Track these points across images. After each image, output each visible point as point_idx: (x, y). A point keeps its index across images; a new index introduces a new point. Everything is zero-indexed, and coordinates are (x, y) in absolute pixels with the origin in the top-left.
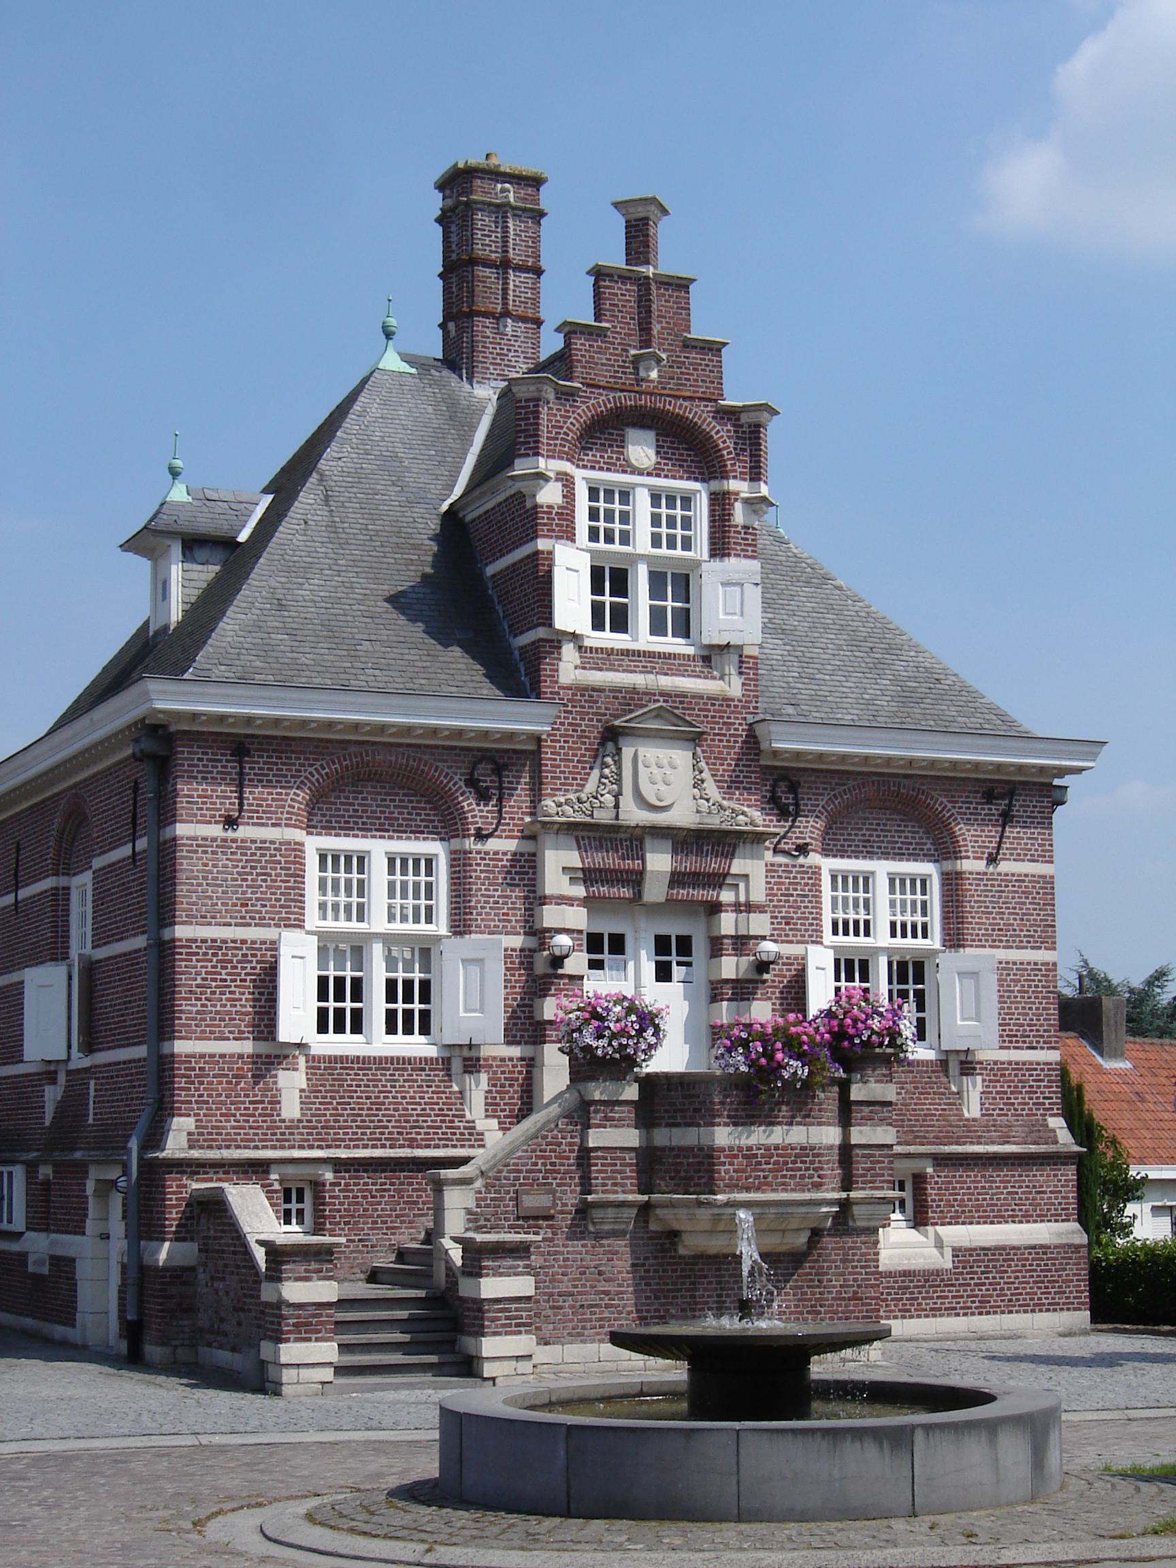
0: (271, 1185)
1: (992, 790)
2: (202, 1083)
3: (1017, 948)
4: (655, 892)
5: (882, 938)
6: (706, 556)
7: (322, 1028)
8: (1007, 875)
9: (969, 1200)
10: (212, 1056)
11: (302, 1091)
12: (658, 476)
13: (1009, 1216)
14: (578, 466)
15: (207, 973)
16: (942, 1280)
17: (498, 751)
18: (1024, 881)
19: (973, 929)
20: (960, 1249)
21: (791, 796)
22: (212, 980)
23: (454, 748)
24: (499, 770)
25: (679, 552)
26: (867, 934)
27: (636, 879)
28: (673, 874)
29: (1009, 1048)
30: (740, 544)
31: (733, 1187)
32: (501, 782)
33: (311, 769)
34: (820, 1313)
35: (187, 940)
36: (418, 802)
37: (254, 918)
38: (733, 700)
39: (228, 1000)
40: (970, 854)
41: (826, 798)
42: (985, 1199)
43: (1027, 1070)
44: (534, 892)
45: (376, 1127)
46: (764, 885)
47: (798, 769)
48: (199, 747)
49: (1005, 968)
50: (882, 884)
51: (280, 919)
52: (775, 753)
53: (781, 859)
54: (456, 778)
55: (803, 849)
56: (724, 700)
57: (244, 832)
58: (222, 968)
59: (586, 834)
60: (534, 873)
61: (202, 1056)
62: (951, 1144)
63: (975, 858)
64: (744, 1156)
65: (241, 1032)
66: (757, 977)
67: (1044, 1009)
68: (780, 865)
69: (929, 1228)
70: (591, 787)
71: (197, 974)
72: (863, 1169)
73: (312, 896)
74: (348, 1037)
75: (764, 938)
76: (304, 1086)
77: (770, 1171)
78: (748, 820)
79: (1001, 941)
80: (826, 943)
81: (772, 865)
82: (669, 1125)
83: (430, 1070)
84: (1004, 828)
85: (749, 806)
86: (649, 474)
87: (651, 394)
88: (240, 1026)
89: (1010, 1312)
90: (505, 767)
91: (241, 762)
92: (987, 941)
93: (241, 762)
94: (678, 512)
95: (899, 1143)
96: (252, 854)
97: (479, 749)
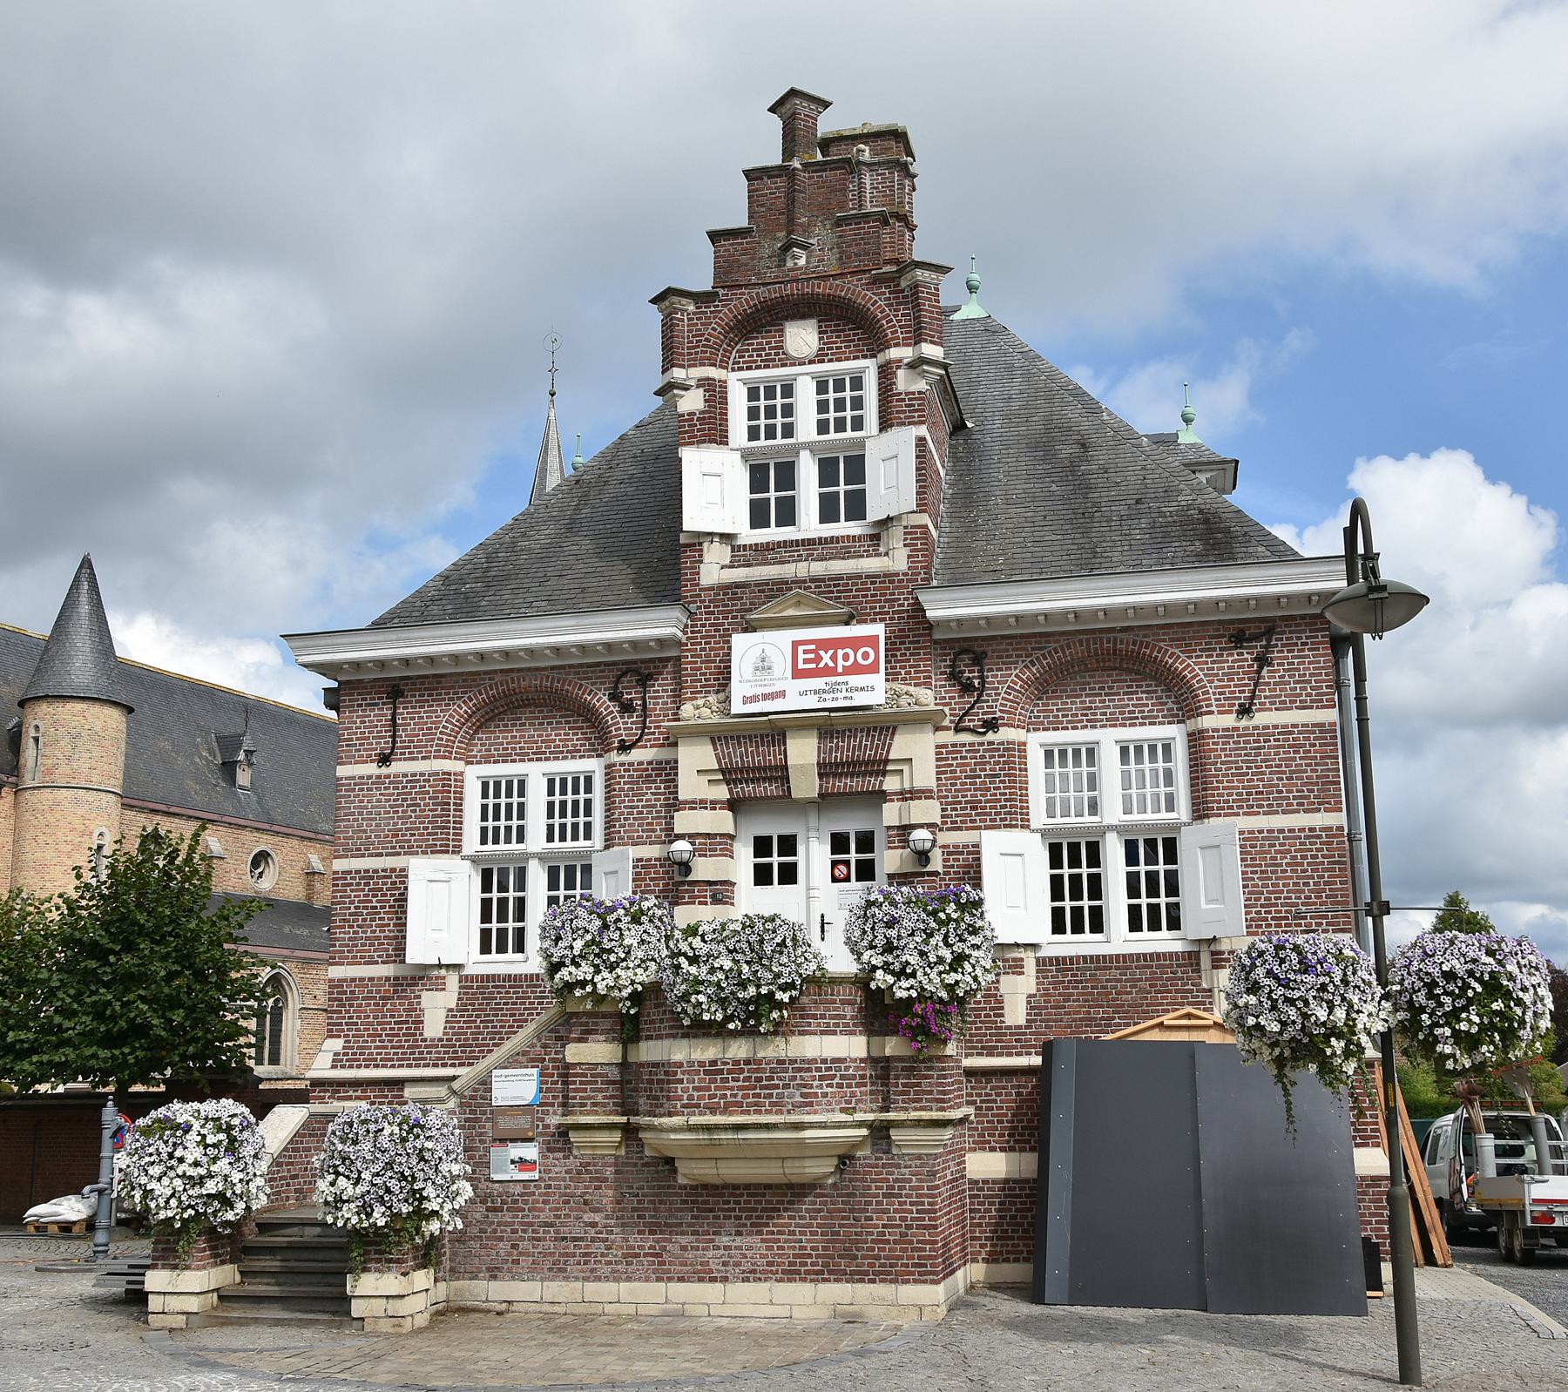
1: (1242, 631)
3: (1284, 812)
4: (805, 785)
11: (450, 1010)
12: (822, 361)
17: (643, 661)
18: (1291, 733)
23: (598, 664)
25: (849, 434)
27: (781, 773)
31: (692, 1106)
34: (856, 1257)
40: (1214, 708)
41: (1021, 665)
47: (984, 639)
49: (1248, 838)
50: (1109, 757)
52: (945, 623)
53: (966, 738)
55: (991, 725)
56: (885, 575)
57: (397, 767)
61: (353, 980)
63: (1220, 713)
64: (706, 1072)
67: (1326, 883)
71: (352, 902)
76: (453, 1006)
82: (649, 1038)
85: (916, 685)
86: (811, 362)
87: (797, 281)
90: (650, 677)
91: (394, 703)
92: (1241, 807)
93: (394, 703)
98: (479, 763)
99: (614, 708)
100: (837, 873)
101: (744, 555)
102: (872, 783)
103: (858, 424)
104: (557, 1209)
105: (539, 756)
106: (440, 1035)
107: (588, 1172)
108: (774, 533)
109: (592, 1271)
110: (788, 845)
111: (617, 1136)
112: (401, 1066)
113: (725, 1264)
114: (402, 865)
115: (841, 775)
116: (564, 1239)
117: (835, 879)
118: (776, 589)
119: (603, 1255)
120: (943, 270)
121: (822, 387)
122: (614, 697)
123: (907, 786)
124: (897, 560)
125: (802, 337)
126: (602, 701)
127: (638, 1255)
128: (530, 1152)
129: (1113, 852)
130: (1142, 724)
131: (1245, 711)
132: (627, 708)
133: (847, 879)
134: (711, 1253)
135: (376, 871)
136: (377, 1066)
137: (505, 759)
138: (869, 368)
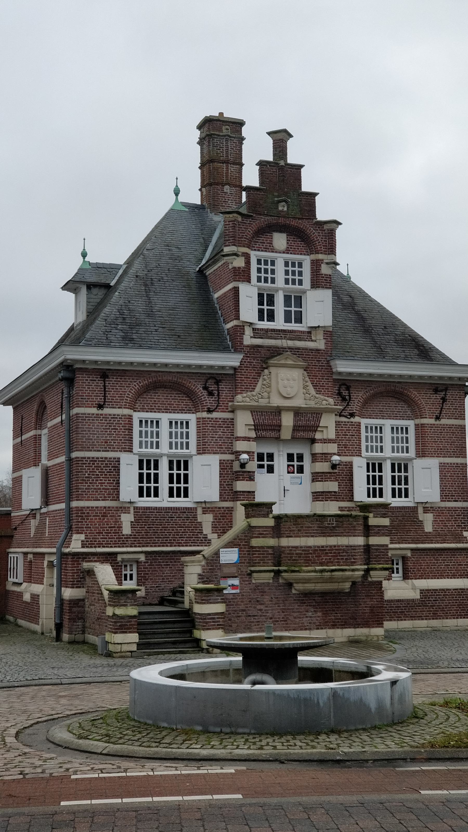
0: (118, 563)
2: (88, 519)
3: (449, 457)
4: (286, 434)
5: (387, 453)
6: (309, 287)
7: (141, 495)
8: (444, 425)
9: (427, 568)
10: (92, 507)
11: (132, 522)
12: (288, 253)
13: (446, 575)
14: (252, 250)
15: (90, 472)
16: (415, 604)
17: (217, 374)
19: (429, 449)
20: (423, 590)
21: (347, 392)
22: (93, 475)
24: (217, 382)
25: (297, 286)
26: (382, 451)
27: (278, 428)
28: (294, 426)
29: (445, 501)
30: (324, 282)
32: (218, 388)
33: (135, 383)
35: (81, 458)
36: (182, 397)
37: (110, 448)
38: (321, 350)
39: (99, 483)
41: (363, 392)
42: (434, 568)
43: (454, 511)
44: (233, 435)
45: (164, 538)
46: (335, 431)
48: (86, 375)
51: (122, 448)
52: (340, 373)
54: (199, 386)
55: (352, 415)
57: (106, 411)
58: (97, 469)
59: (254, 411)
60: (233, 427)
61: (88, 507)
62: (419, 543)
65: (104, 497)
66: (332, 471)
67: (461, 484)
68: (342, 422)
69: (410, 581)
70: (258, 389)
71: (86, 472)
72: (375, 555)
73: (136, 439)
74: (152, 498)
75: (335, 454)
76: (133, 520)
77: (332, 556)
78: (327, 403)
79: (441, 454)
80: (363, 455)
81: (339, 422)
82: (288, 537)
83: (188, 512)
84: (443, 404)
85: (328, 397)
86: (284, 253)
87: (284, 217)
88: (104, 494)
89: (447, 618)
91: (104, 381)
93: (104, 381)
94: (297, 269)
95: (391, 543)
96: (110, 420)
97: (209, 374)
98: (139, 411)
99: (205, 393)
100: (289, 469)
101: (258, 333)
102: (311, 435)
103: (301, 282)
104: (247, 604)
105: (167, 411)
106: (130, 533)
107: (258, 589)
108: (265, 324)
109: (261, 628)
110: (271, 457)
111: (272, 574)
112: (115, 547)
113: (310, 623)
114: (118, 456)
115: (299, 430)
116: (249, 616)
117: (289, 472)
118: (276, 352)
119: (265, 622)
120: (339, 224)
121: (286, 264)
122: (205, 388)
123: (325, 437)
124: (319, 343)
125: (280, 240)
126: (199, 389)
127: (278, 621)
128: (236, 582)
129: (387, 467)
130: (400, 419)
131: (438, 418)
132: (211, 394)
133: (293, 473)
134: (304, 619)
135: (98, 458)
136: (104, 547)
137: (151, 410)
138: (307, 260)
